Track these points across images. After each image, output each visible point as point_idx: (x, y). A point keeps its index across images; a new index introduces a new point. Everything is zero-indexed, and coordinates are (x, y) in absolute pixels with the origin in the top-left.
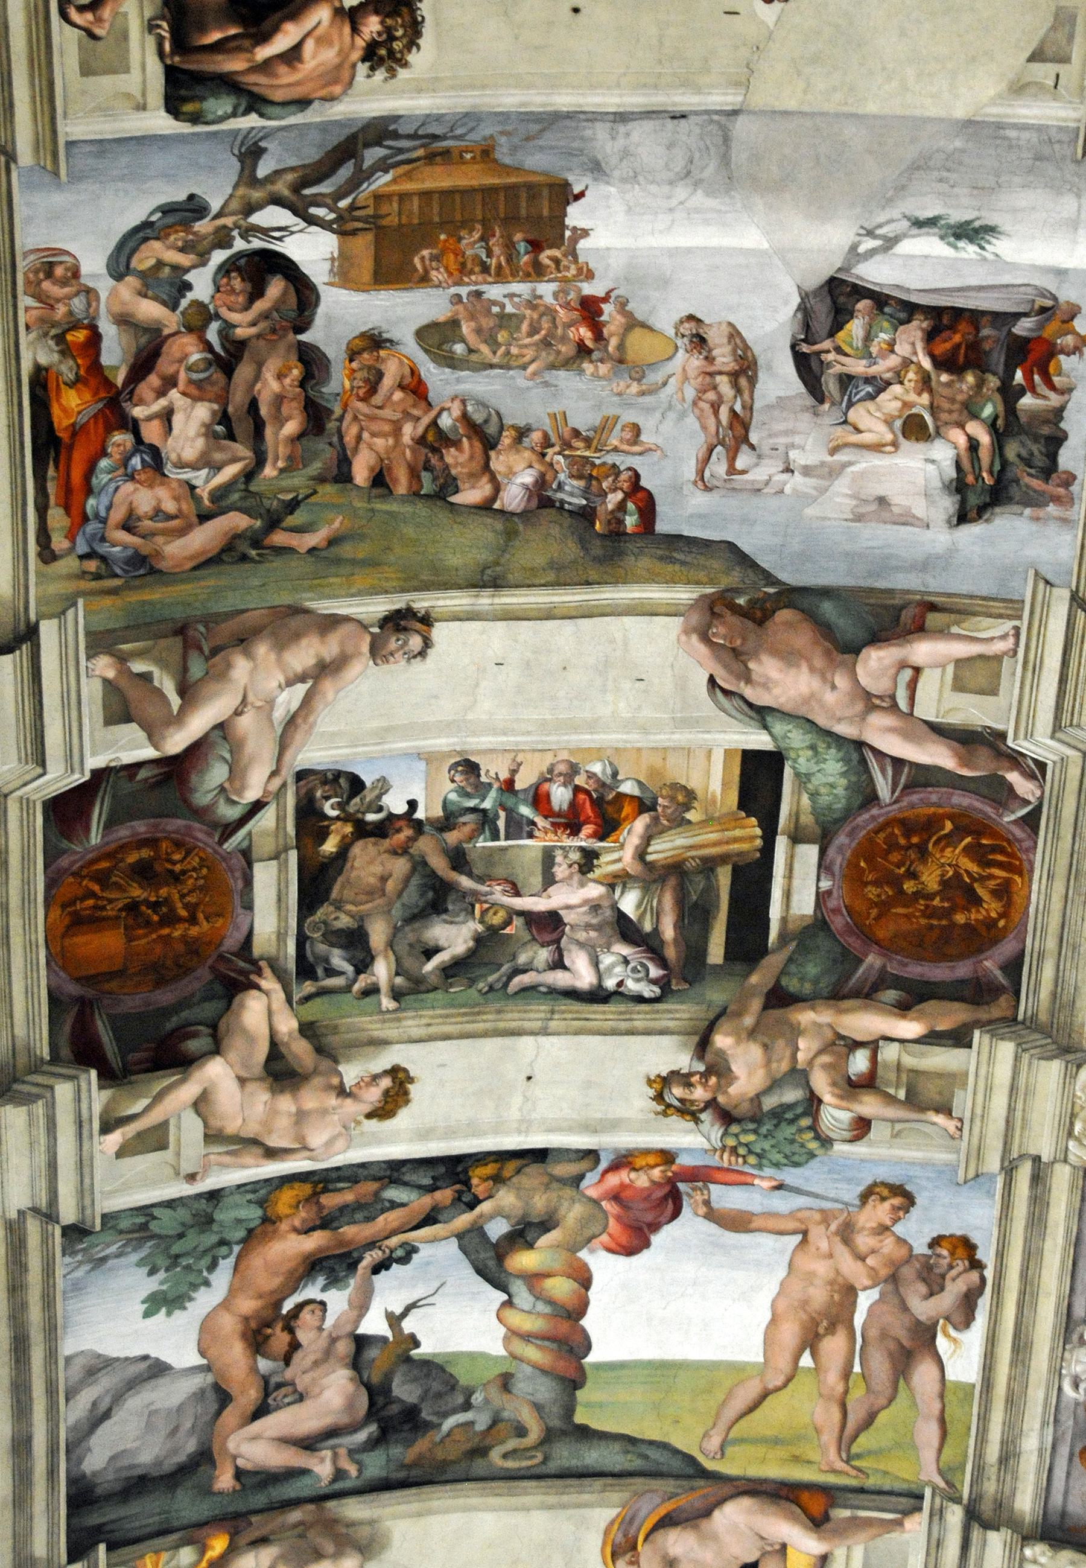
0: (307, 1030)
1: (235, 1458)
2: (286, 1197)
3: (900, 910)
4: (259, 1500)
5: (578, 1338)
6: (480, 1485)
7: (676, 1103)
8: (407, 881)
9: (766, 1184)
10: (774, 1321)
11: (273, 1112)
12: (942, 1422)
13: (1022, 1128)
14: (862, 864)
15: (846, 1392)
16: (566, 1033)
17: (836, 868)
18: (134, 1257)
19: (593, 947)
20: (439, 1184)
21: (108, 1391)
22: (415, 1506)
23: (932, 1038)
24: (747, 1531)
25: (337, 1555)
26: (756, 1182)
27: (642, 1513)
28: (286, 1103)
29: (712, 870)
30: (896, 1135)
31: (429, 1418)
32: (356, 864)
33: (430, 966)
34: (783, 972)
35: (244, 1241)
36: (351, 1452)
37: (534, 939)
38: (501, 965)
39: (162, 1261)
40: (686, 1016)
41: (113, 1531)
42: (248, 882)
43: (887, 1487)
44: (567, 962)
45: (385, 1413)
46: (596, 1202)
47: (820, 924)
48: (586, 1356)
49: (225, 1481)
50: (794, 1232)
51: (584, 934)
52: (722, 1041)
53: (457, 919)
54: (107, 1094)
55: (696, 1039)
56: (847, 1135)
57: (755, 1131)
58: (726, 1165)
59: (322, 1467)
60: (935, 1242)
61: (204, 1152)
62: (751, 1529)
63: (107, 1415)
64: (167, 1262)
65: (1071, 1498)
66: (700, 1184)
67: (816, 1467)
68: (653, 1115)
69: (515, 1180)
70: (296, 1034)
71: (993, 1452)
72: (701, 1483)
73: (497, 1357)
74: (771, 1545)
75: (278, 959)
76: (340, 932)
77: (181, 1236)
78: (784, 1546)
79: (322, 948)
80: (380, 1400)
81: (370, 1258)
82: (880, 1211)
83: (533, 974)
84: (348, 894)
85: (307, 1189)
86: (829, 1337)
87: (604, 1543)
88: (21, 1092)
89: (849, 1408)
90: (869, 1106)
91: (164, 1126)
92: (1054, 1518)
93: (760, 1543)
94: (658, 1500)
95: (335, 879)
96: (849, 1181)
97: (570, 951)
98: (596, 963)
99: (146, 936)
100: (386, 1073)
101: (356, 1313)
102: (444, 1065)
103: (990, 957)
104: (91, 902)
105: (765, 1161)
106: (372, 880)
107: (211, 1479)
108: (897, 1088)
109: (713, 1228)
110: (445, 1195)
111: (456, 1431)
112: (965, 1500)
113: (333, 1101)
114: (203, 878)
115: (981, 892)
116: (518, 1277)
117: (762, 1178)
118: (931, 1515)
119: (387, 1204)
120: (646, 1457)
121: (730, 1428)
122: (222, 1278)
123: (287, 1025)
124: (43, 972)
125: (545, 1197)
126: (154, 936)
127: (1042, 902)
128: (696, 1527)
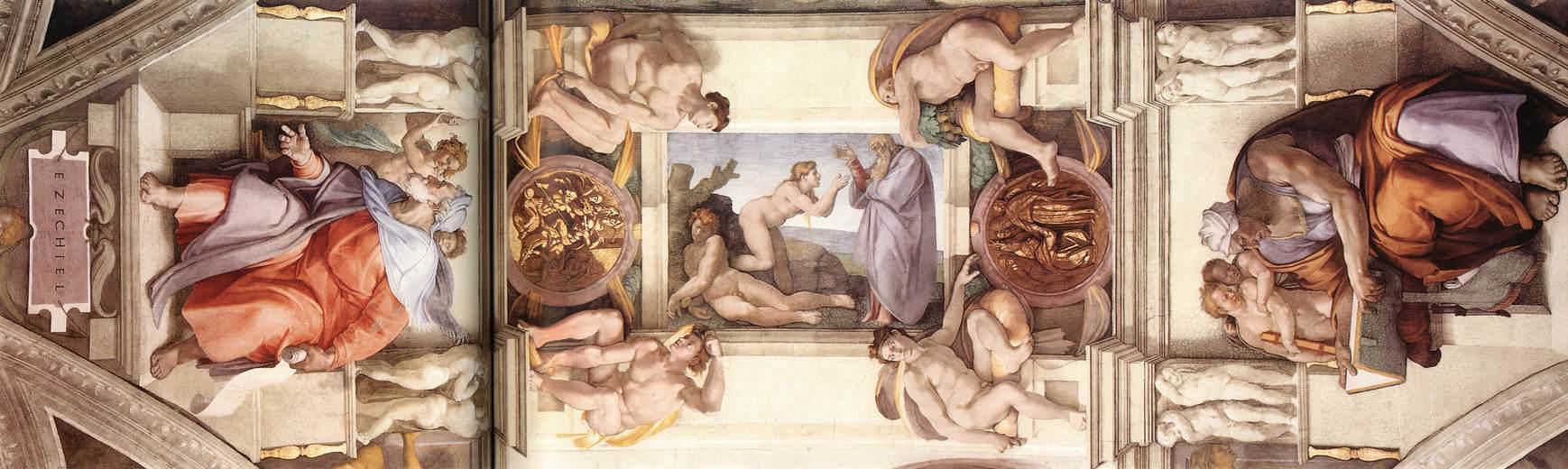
22: (736, 31)
24: (964, 53)
25: (683, 63)
62: (968, 52)
72: (932, 13)
74: (983, 65)
78: (992, 64)
128: (931, 54)
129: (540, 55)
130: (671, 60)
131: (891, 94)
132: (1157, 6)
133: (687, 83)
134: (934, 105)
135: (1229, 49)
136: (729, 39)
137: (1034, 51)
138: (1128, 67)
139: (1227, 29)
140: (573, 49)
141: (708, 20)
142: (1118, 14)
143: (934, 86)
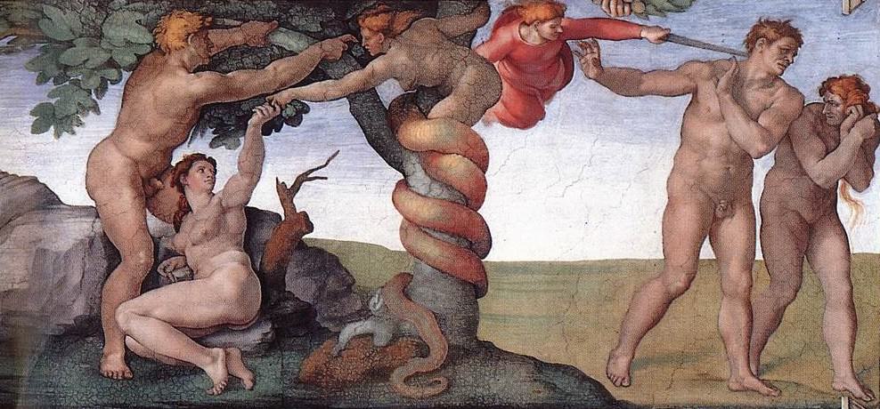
9: (653, 36)
12: (852, 307)
18: (24, 58)
26: (644, 34)
35: (132, 68)
46: (489, 63)
58: (613, 16)
60: (825, 88)
77: (70, 44)
82: (767, 58)
101: (247, 181)
105: (650, 8)
109: (604, 92)
110: (334, 46)
122: (110, 104)
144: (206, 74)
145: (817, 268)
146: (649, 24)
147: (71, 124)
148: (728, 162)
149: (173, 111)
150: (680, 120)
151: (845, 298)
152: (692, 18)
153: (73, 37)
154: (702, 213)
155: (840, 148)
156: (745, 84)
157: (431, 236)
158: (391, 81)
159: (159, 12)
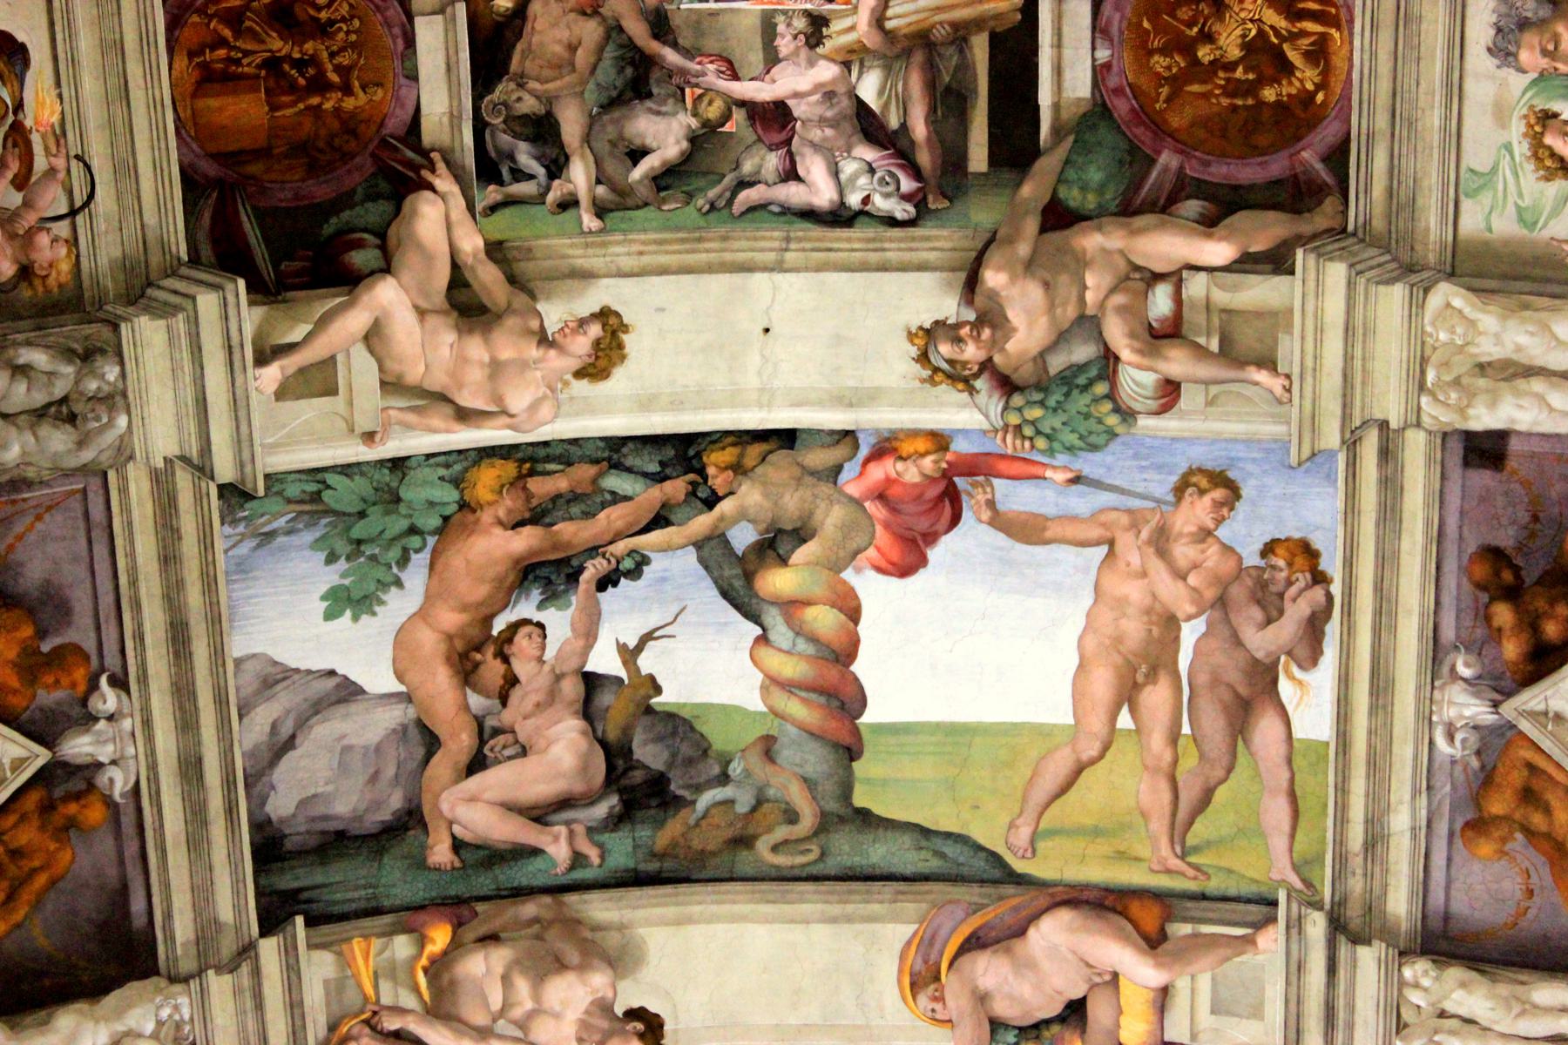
0: (495, 250)
1: (451, 823)
2: (487, 478)
3: (1196, 88)
4: (484, 882)
5: (850, 689)
6: (749, 886)
7: (945, 366)
8: (600, 50)
9: (1060, 477)
10: (1082, 667)
11: (462, 360)
13: (1363, 383)
14: (1146, 24)
15: (1175, 761)
16: (807, 269)
17: (1114, 30)
18: (308, 537)
19: (831, 150)
20: (668, 471)
21: (288, 712)
22: (671, 911)
23: (1247, 263)
24: (1070, 956)
25: (582, 968)
26: (1049, 474)
27: (943, 933)
28: (476, 348)
29: (965, 39)
30: (1210, 403)
31: (680, 792)
32: (538, 26)
33: (638, 173)
34: (1060, 180)
35: (439, 531)
36: (590, 831)
37: (760, 140)
38: (724, 176)
39: (342, 547)
40: (949, 245)
41: (309, 901)
42: (410, 41)
43: (1232, 892)
44: (801, 172)
45: (624, 782)
46: (857, 503)
47: (1099, 111)
48: (860, 714)
49: (441, 853)
50: (1098, 543)
51: (819, 132)
52: (993, 278)
53: (664, 109)
54: (259, 312)
55: (963, 276)
56: (1153, 405)
57: (1042, 403)
58: (1010, 451)
59: (557, 847)
60: (1269, 549)
61: (381, 404)
62: (1074, 953)
63: (290, 744)
64: (349, 548)
65: (1453, 893)
66: (981, 478)
67: (1145, 865)
68: (917, 384)
69: (759, 470)
70: (482, 255)
71: (1356, 836)
72: (1010, 890)
73: (756, 713)
74: (1099, 974)
75: (453, 150)
76: (525, 119)
77: (362, 515)
78: (1115, 975)
79: (505, 139)
80: (620, 763)
81: (594, 569)
82: (1198, 510)
83: (761, 188)
84: (530, 67)
85: (509, 469)
86: (1148, 689)
87: (900, 971)
88: (156, 300)
89: (1180, 784)
90: (1177, 363)
91: (331, 361)
92: (1435, 923)
93: (1088, 971)
94: (960, 914)
95: (514, 46)
96: (1159, 468)
97: (803, 155)
98: (835, 173)
99: (294, 104)
100: (594, 316)
101: (581, 643)
102: (662, 310)
103: (1309, 145)
104: (222, 53)
105: (1056, 445)
106: (558, 49)
107: (424, 848)
108: (1208, 335)
109: (1000, 539)
110: (676, 488)
111: (713, 811)
112: (1327, 906)
113: (534, 352)
114: (355, 32)
115: (1293, 56)
116: (772, 603)
117: (1054, 467)
118: (1288, 928)
119: (608, 497)
120: (942, 855)
121: (1041, 814)
122: (416, 577)
123: (471, 243)
124: (173, 143)
125: (797, 495)
126: (301, 106)
127: (1367, 64)
128: (1008, 951)
129: (335, 989)
130: (561, 966)
131: (938, 1006)
132: (1403, 928)
133: (590, 999)
134: (1014, 1027)
135: (1523, 1013)
136: (657, 925)
137: (1189, 964)
138: (1351, 1008)
139: (1522, 983)
140: (394, 969)
141: (620, 899)
142: (1336, 929)
143: (1011, 997)
144: (527, 530)
145: (1254, 749)
146: (1056, 463)
147: (371, 604)
148: (1151, 623)
149: (492, 572)
150: (1094, 572)
151: (1285, 785)
152: (1109, 459)
153: (365, 506)
154: (1120, 677)
155: (1283, 620)
156: (1172, 538)
157: (796, 695)
158: (744, 524)
159: (465, 464)
